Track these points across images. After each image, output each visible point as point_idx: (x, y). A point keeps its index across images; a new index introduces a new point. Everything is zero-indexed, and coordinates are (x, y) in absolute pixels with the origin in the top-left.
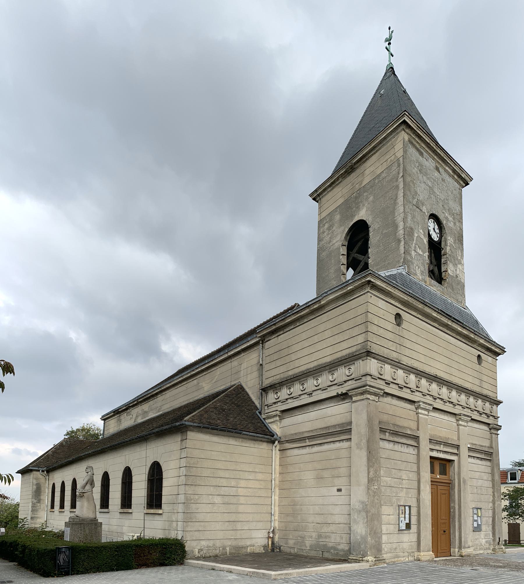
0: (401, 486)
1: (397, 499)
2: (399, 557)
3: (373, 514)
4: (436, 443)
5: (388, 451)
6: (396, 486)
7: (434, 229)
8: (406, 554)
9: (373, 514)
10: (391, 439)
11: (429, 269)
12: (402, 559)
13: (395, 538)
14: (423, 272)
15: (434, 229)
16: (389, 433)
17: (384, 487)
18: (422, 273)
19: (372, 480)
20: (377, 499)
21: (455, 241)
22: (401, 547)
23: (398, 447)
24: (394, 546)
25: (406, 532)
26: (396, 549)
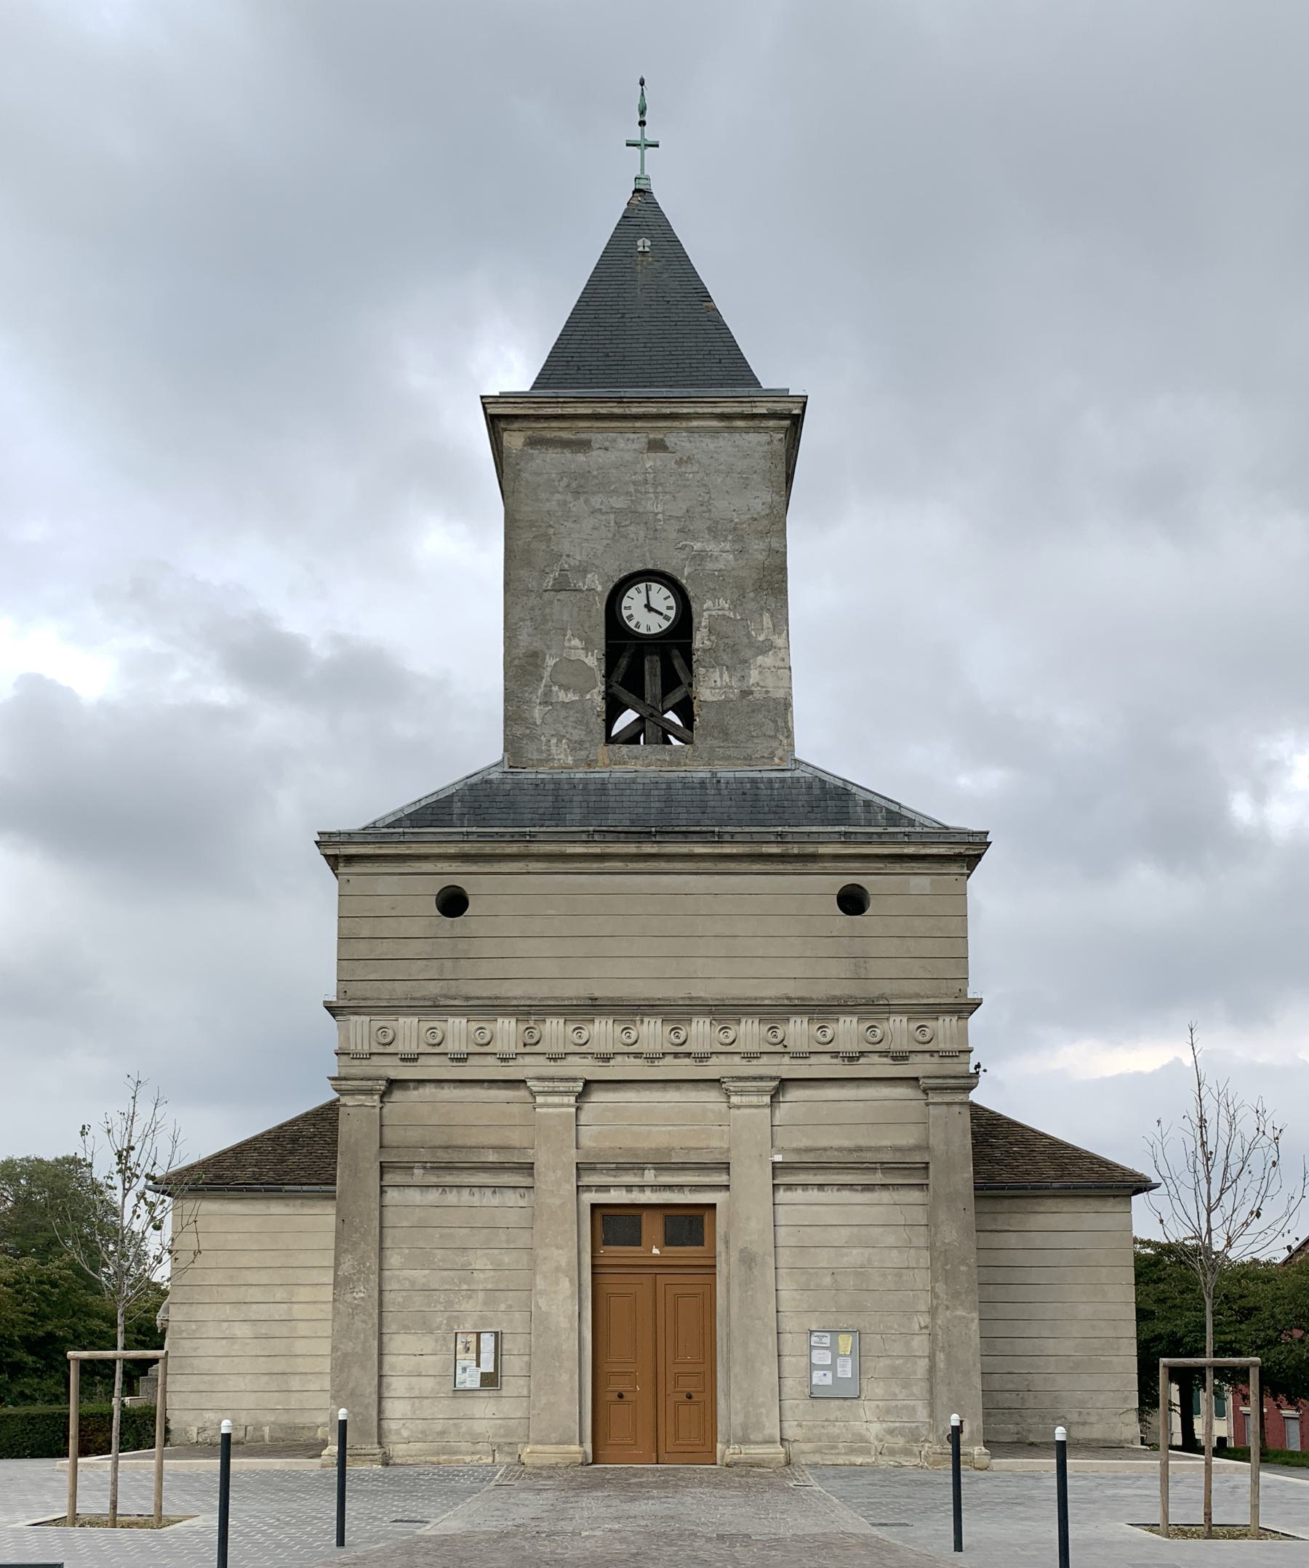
0: (465, 1287)
1: (449, 1319)
2: (455, 1453)
4: (617, 1169)
5: (417, 1210)
6: (447, 1287)
7: (648, 606)
8: (487, 1447)
10: (432, 1179)
12: (468, 1459)
14: (581, 742)
15: (648, 606)
16: (424, 1168)
17: (405, 1294)
18: (576, 746)
19: (348, 1279)
20: (364, 1322)
22: (463, 1430)
23: (452, 1197)
24: (438, 1426)
25: (481, 1394)
26: (443, 1433)
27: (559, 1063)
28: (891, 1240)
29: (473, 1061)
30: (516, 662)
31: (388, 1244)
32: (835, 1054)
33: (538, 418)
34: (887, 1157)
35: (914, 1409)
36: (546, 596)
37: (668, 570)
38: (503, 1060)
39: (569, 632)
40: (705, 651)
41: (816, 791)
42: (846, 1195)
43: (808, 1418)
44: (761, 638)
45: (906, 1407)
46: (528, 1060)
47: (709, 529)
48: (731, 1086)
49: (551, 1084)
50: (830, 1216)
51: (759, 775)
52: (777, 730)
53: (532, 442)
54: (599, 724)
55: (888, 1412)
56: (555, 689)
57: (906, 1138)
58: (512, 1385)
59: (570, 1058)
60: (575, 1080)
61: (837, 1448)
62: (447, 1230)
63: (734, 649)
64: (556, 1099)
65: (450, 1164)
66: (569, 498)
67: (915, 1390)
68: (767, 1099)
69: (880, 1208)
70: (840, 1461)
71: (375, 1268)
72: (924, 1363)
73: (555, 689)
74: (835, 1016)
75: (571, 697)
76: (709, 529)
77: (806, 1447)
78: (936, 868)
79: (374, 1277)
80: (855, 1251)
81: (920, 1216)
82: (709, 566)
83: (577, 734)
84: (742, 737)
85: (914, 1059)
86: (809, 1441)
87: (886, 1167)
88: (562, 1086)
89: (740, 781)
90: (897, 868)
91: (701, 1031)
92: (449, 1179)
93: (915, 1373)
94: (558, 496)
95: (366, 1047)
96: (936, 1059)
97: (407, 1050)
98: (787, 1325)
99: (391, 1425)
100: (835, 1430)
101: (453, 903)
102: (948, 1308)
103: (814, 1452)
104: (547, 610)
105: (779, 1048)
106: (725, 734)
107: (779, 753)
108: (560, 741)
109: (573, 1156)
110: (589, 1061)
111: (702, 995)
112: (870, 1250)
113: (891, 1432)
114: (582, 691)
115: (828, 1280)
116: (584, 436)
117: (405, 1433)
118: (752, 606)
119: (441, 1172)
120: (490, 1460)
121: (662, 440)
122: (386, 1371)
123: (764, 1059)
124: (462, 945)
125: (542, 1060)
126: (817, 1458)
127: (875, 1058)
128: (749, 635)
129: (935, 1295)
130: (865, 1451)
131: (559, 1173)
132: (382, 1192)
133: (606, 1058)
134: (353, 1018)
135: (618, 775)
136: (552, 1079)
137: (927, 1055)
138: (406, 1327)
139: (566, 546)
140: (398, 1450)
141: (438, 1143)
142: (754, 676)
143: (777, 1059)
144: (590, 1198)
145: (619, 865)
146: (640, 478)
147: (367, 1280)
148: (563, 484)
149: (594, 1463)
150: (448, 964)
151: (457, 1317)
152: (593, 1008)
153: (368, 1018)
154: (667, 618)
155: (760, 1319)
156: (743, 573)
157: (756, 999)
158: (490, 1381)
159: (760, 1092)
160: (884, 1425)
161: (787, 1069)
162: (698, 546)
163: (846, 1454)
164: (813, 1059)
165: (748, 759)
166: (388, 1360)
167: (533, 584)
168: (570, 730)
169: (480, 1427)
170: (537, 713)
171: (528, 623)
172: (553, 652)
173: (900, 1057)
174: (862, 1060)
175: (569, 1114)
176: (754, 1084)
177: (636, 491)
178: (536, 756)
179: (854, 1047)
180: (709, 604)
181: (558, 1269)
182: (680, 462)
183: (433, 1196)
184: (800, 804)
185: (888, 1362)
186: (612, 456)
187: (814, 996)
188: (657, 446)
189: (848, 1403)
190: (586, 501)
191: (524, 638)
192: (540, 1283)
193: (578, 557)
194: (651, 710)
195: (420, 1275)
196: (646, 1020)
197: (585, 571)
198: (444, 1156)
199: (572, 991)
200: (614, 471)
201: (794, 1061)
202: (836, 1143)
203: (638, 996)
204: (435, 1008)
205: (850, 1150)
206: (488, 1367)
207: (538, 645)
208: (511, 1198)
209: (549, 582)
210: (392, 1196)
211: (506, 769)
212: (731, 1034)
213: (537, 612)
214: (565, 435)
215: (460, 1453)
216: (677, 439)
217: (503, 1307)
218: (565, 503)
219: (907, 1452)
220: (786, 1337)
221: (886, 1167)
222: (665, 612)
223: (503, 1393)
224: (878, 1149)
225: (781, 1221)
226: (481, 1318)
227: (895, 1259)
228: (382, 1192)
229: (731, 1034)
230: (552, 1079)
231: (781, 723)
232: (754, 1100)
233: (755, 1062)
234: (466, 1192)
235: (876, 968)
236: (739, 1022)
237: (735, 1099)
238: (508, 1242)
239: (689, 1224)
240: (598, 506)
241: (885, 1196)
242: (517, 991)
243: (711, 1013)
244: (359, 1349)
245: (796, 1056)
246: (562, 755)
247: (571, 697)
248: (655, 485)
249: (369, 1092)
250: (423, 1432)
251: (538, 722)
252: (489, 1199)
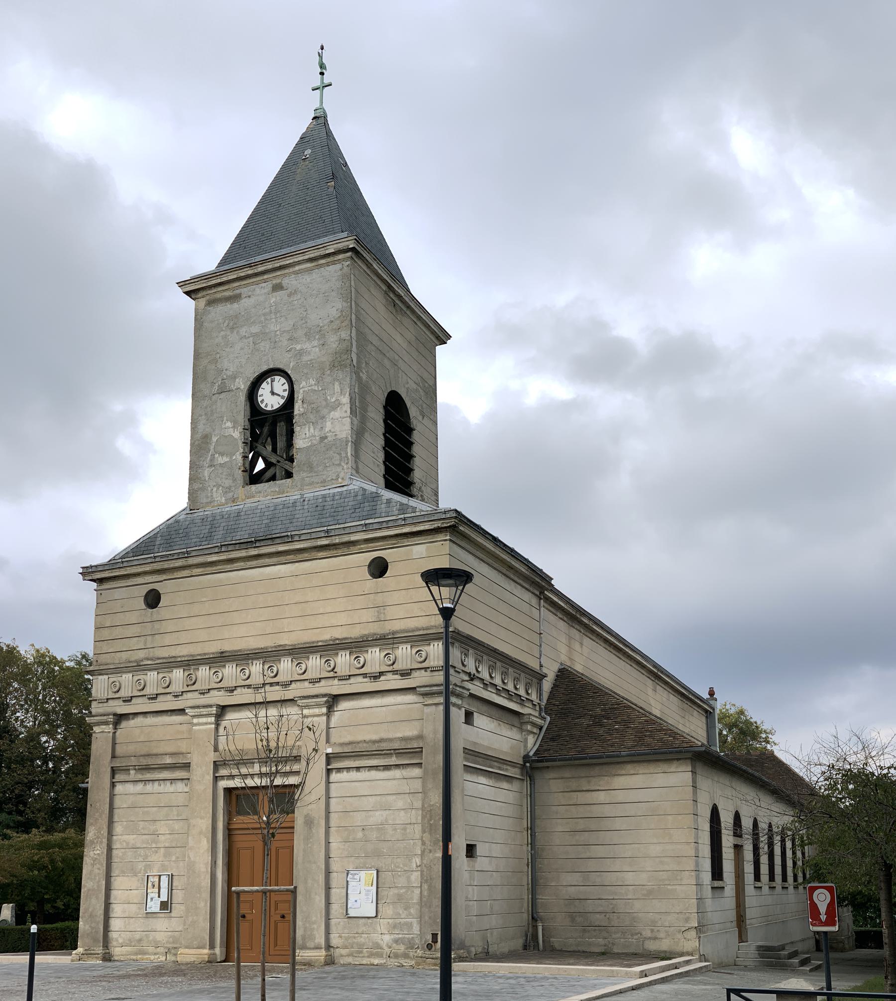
0: (154, 846)
1: (146, 866)
2: (145, 953)
3: (89, 890)
5: (131, 797)
7: (273, 393)
9: (89, 890)
10: (140, 777)
12: (152, 957)
13: (138, 925)
14: (230, 488)
15: (273, 393)
17: (123, 850)
22: (151, 938)
23: (149, 787)
24: (137, 936)
26: (140, 940)
27: (206, 696)
28: (400, 804)
29: (160, 698)
30: (197, 443)
31: (116, 818)
32: (365, 675)
33: (210, 287)
34: (396, 745)
35: (410, 926)
36: (214, 397)
38: (176, 696)
40: (300, 415)
41: (360, 498)
42: (374, 774)
43: (346, 931)
44: (333, 400)
45: (406, 924)
46: (189, 695)
47: (306, 334)
48: (300, 702)
49: (198, 710)
50: (363, 789)
51: (327, 492)
52: (341, 460)
53: (210, 303)
54: (239, 475)
55: (395, 927)
56: (217, 456)
57: (410, 731)
58: (178, 909)
59: (212, 692)
60: (211, 706)
61: (361, 952)
62: (146, 809)
63: (317, 411)
64: (204, 720)
65: (149, 767)
66: (228, 333)
67: (412, 911)
68: (324, 710)
69: (394, 782)
70: (364, 962)
71: (106, 834)
72: (418, 891)
73: (217, 456)
74: (366, 649)
75: (226, 459)
77: (344, 952)
78: (430, 538)
79: (105, 841)
80: (378, 813)
81: (417, 785)
82: (305, 358)
83: (228, 483)
84: (320, 468)
85: (415, 674)
86: (346, 947)
87: (398, 753)
88: (204, 711)
90: (406, 542)
91: (286, 666)
92: (149, 776)
93: (412, 899)
94: (222, 333)
95: (106, 696)
96: (428, 673)
97: (126, 695)
98: (334, 866)
99: (113, 935)
100: (361, 940)
101: (153, 599)
102: (430, 851)
103: (348, 955)
104: (214, 407)
105: (332, 674)
106: (311, 468)
107: (342, 475)
108: (218, 488)
109: (212, 756)
110: (222, 693)
111: (287, 642)
112: (387, 812)
113: (396, 941)
115: (360, 835)
116: (238, 292)
117: (121, 941)
118: (328, 379)
119: (144, 772)
120: (164, 958)
121: (280, 283)
122: (112, 900)
123: (323, 682)
124: (157, 625)
125: (196, 694)
126: (350, 960)
127: (390, 676)
129: (423, 843)
130: (380, 955)
131: (204, 768)
132: (113, 785)
133: (231, 690)
134: (100, 677)
135: (249, 505)
136: (198, 707)
137: (423, 671)
138: (123, 872)
139: (225, 364)
140: (117, 951)
141: (143, 753)
142: (328, 426)
143: (330, 682)
144: (223, 784)
145: (241, 564)
146: (267, 310)
147: (101, 842)
148: (225, 324)
149: (224, 961)
150: (149, 638)
151: (149, 865)
152: (221, 659)
153: (106, 677)
154: (283, 397)
155: (315, 863)
156: (323, 359)
157: (313, 642)
158: (164, 906)
159: (318, 705)
160: (392, 937)
161: (336, 688)
162: (298, 347)
163: (368, 957)
164: (352, 680)
166: (114, 893)
167: (207, 392)
168: (224, 480)
169: (161, 937)
172: (216, 432)
173: (405, 674)
174: (382, 678)
175: (210, 729)
176: (314, 700)
177: (266, 319)
178: (205, 500)
179: (377, 669)
180: (304, 383)
181: (201, 833)
182: (289, 295)
183: (140, 787)
184: (348, 508)
185: (396, 891)
186: (252, 301)
187: (353, 636)
188: (278, 287)
189: (370, 921)
190: (238, 332)
191: (201, 427)
192: (191, 843)
194: (279, 459)
195: (131, 838)
196: (254, 662)
197: (235, 378)
198: (144, 761)
199: (213, 648)
200: (253, 310)
201: (341, 682)
202: (368, 737)
203: (251, 647)
204: (138, 667)
205: (374, 742)
206: (164, 898)
207: (208, 430)
208: (180, 786)
209: (216, 388)
210: (119, 788)
212: (303, 666)
213: (209, 409)
214: (227, 294)
215: (149, 954)
216: (290, 281)
217: (174, 858)
218: (225, 337)
219: (406, 956)
220: (334, 876)
221: (398, 753)
222: (282, 393)
223: (173, 914)
224: (391, 740)
225: (333, 794)
226: (163, 865)
227: (402, 817)
228: (113, 785)
229: (303, 666)
230: (198, 707)
231: (343, 455)
232: (316, 711)
233: (317, 685)
234: (156, 783)
235: (391, 612)
236: (308, 658)
237: (306, 712)
238: (178, 815)
239: (285, 799)
240: (244, 334)
241: (397, 773)
242: (183, 652)
243: (290, 654)
244: (95, 887)
245: (342, 679)
246: (219, 497)
247: (226, 459)
248: (276, 313)
249: (106, 723)
250: (130, 940)
252: (168, 787)
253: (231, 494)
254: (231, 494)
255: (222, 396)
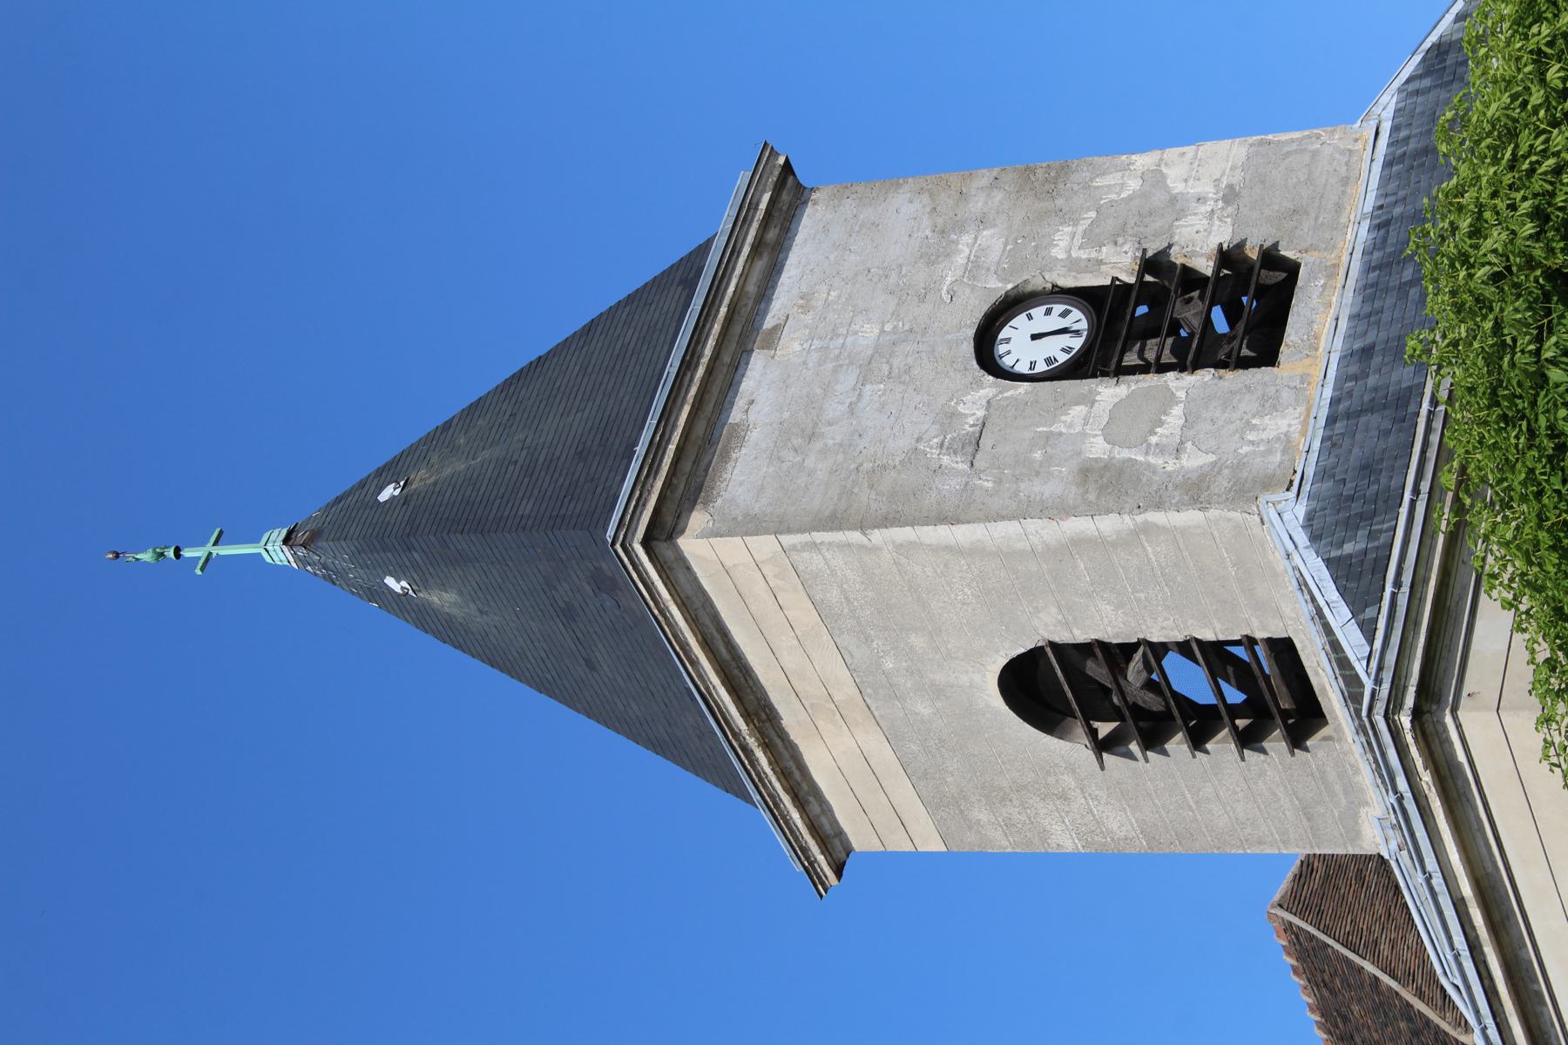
11: (1244, 364)
14: (1264, 399)
18: (1270, 404)
21: (1067, 216)
30: (1092, 497)
37: (985, 308)
39: (1058, 427)
47: (930, 263)
66: (818, 445)
76: (930, 263)
89: (1385, 180)
108: (1254, 428)
114: (1171, 400)
128: (1130, 198)
165: (1345, 181)
167: (954, 484)
170: (1194, 460)
171: (1023, 486)
178: (1278, 457)
190: (830, 424)
191: (1048, 489)
193: (924, 427)
197: (954, 415)
211: (1292, 494)
218: (825, 451)
240: (844, 408)
251: (1212, 458)
253: (1286, 395)
254: (1286, 395)
255: (986, 442)
